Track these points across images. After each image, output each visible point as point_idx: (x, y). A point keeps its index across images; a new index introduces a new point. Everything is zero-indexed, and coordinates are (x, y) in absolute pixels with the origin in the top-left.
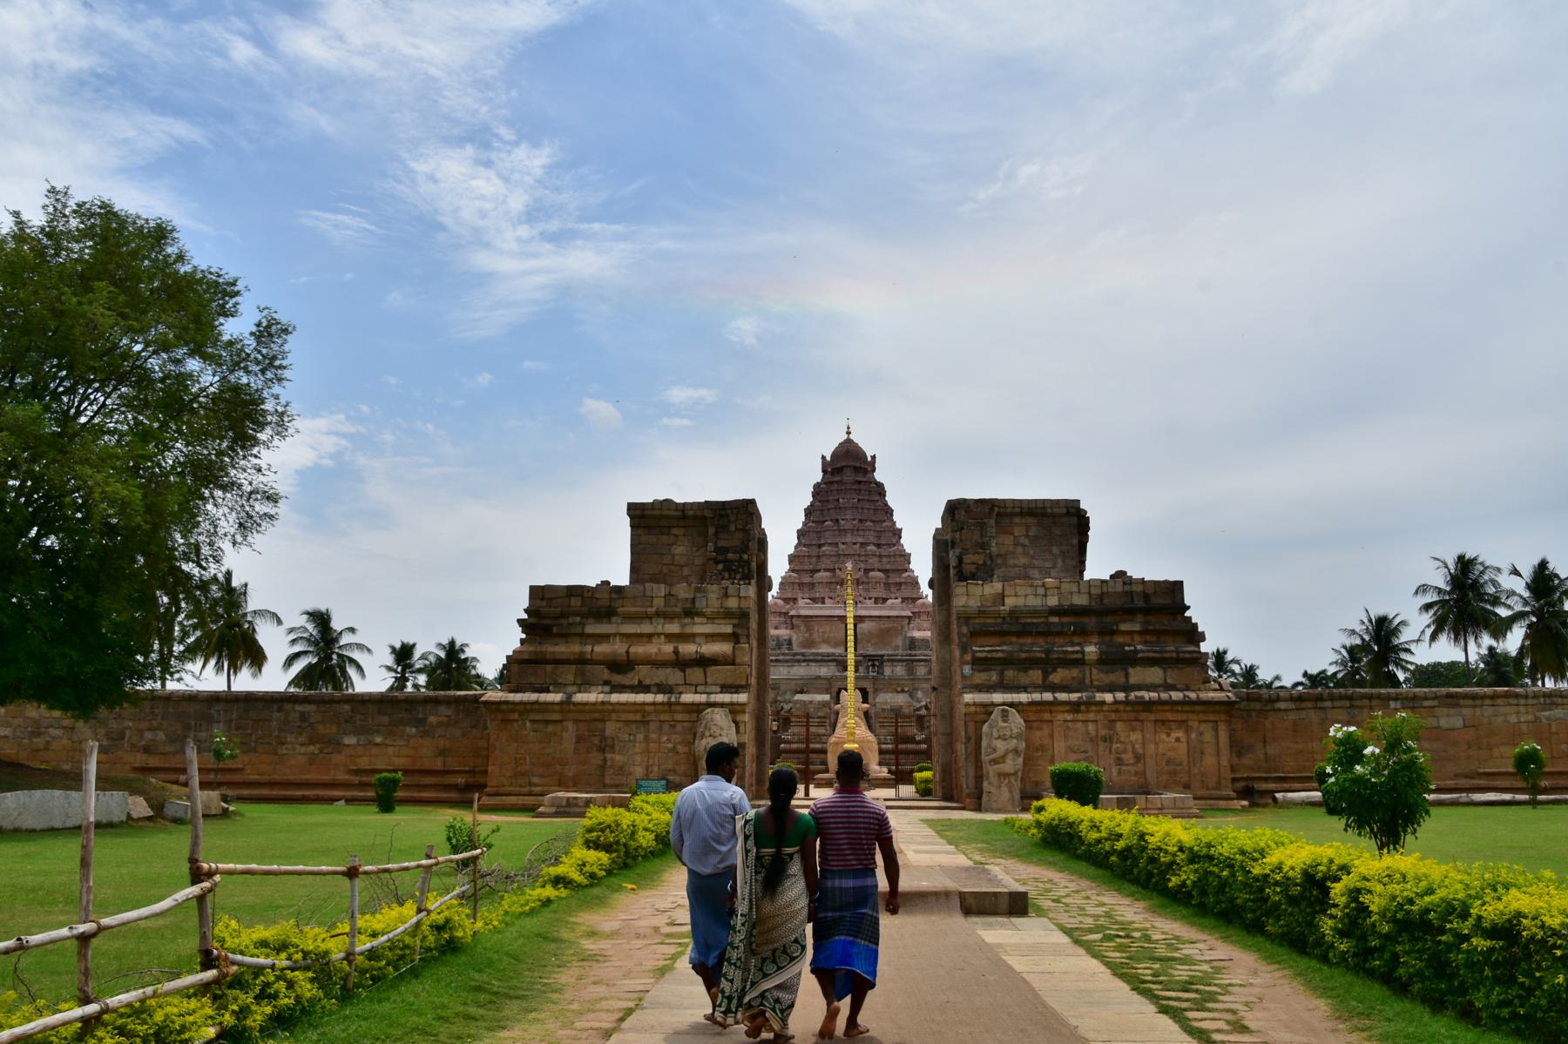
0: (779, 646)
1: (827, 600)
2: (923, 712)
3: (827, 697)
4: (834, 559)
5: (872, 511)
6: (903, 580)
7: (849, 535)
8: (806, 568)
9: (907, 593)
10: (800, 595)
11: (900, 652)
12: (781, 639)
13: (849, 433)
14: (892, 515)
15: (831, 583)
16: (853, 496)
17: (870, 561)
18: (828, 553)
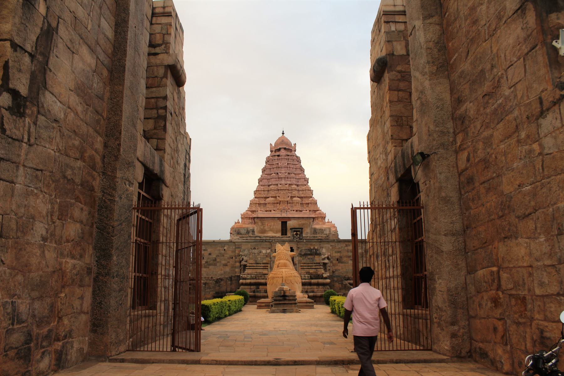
0: (248, 232)
1: (272, 211)
2: (326, 261)
3: (269, 251)
4: (276, 192)
5: (294, 169)
6: (309, 202)
7: (283, 180)
8: (262, 196)
9: (312, 208)
10: (259, 209)
11: (309, 235)
12: (249, 229)
13: (283, 134)
14: (304, 172)
15: (274, 203)
16: (285, 162)
17: (294, 193)
18: (273, 189)
